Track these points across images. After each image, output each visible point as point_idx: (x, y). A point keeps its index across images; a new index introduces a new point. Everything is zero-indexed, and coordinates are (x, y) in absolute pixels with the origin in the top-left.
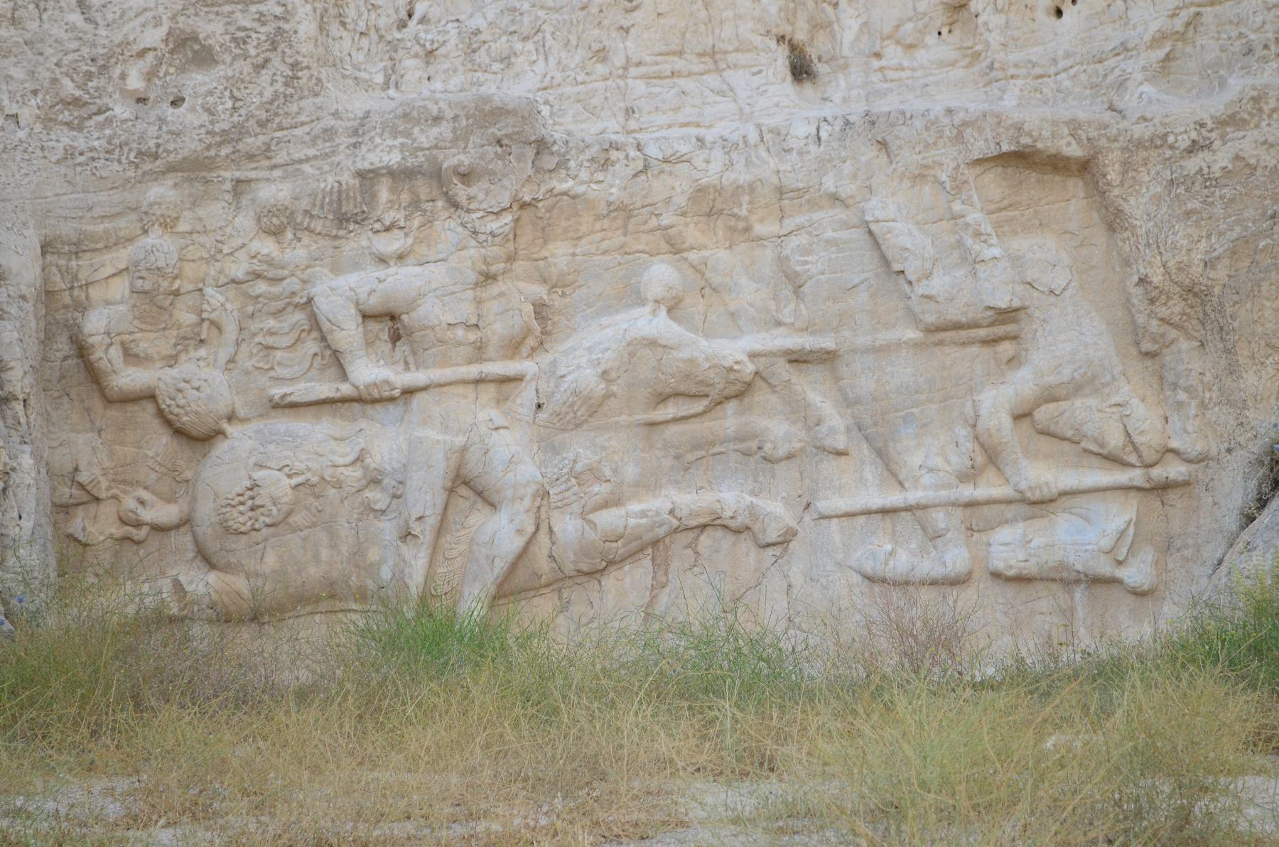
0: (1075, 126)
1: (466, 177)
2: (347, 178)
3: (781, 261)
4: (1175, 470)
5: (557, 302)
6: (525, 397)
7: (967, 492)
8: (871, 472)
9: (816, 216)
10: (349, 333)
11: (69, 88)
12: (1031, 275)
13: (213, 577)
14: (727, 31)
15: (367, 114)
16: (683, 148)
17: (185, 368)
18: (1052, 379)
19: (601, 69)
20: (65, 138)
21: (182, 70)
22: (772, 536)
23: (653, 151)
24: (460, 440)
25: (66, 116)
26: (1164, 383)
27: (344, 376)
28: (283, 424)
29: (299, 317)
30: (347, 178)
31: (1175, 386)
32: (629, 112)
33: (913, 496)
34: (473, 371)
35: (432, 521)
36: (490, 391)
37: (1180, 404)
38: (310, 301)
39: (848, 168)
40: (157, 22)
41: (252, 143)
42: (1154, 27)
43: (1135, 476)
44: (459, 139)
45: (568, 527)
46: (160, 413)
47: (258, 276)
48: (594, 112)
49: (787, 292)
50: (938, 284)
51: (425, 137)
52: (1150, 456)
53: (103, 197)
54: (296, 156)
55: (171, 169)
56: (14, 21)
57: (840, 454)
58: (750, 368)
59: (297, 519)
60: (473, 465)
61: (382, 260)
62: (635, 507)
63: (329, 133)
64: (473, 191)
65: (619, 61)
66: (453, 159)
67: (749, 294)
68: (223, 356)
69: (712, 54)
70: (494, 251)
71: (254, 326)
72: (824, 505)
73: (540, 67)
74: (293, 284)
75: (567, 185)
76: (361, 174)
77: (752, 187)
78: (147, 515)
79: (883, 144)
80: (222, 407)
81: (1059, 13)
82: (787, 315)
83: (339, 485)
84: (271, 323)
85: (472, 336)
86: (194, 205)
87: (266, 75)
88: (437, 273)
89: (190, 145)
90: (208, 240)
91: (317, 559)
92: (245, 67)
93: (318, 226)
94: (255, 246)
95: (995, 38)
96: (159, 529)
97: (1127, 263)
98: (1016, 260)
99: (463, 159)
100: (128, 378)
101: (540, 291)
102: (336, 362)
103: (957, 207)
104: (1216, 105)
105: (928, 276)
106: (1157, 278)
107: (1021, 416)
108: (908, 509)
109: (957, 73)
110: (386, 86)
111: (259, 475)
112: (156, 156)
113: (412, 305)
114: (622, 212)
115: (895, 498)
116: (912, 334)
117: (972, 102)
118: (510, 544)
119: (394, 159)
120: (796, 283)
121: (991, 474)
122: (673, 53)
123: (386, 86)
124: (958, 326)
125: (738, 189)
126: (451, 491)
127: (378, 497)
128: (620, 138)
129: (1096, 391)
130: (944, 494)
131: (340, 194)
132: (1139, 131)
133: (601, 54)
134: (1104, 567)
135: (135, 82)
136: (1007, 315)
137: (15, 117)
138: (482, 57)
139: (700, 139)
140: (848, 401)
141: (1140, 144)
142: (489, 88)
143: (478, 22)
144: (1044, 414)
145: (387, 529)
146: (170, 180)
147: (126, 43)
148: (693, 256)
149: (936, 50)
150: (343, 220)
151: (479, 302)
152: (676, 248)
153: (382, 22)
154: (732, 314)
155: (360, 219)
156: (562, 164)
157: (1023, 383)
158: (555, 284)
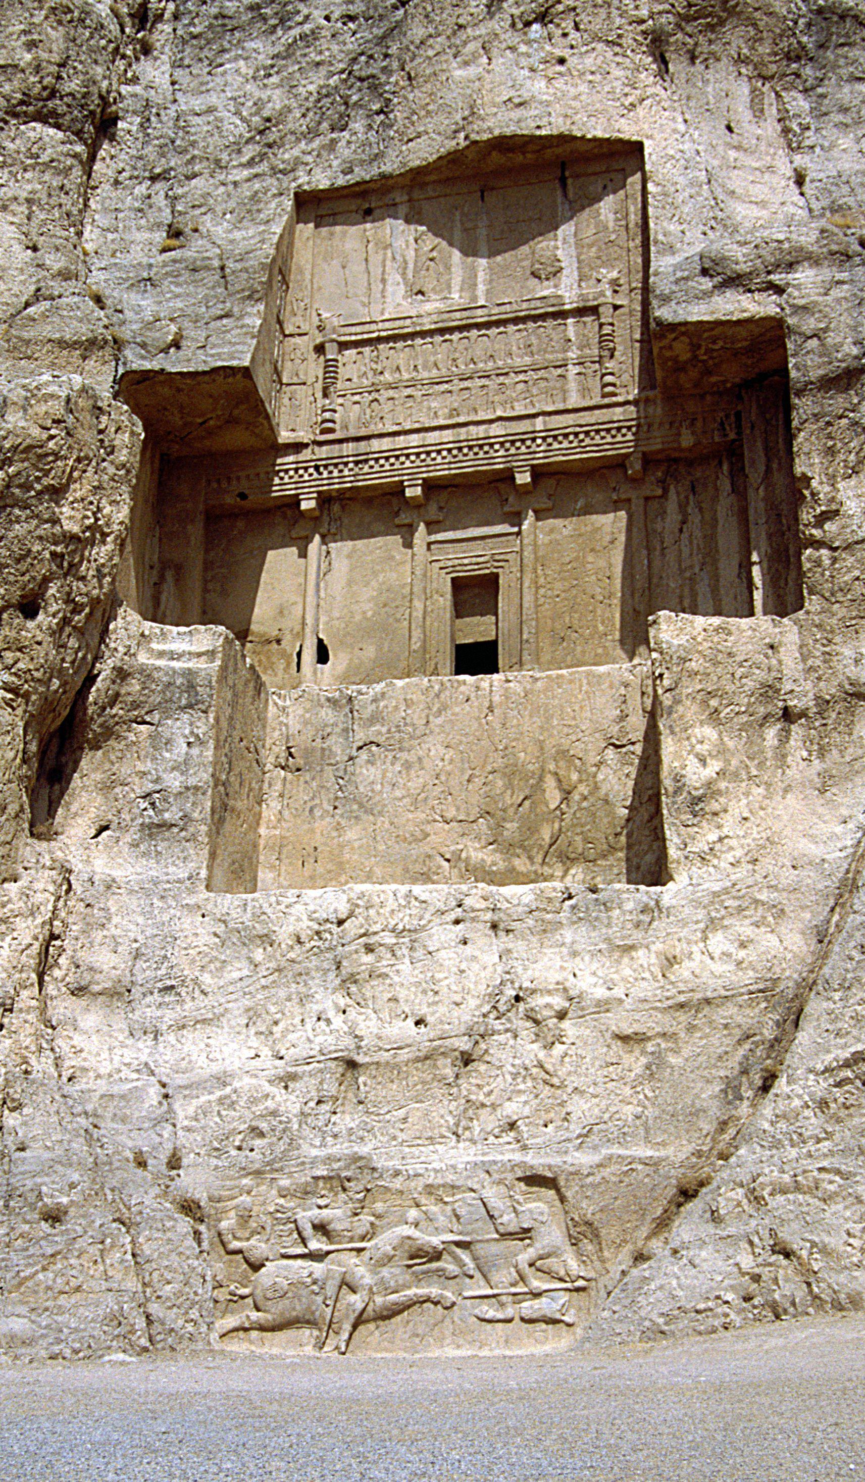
0: (550, 1167)
1: (349, 1180)
2: (309, 1179)
3: (454, 1210)
4: (581, 1283)
5: (377, 1222)
6: (366, 1255)
7: (513, 1290)
8: (482, 1282)
9: (465, 1195)
10: (308, 1231)
11: (216, 1144)
12: (535, 1216)
13: (260, 1314)
14: (436, 1131)
15: (316, 1157)
16: (421, 1171)
17: (253, 1242)
18: (541, 1252)
19: (394, 1143)
20: (215, 1161)
21: (253, 1138)
22: (448, 1305)
23: (411, 1172)
24: (344, 1269)
25: (215, 1154)
26: (579, 1254)
27: (306, 1246)
28: (285, 1262)
29: (292, 1225)
30: (309, 1179)
31: (582, 1255)
32: (403, 1158)
33: (496, 1291)
34: (350, 1246)
35: (334, 1298)
36: (354, 1253)
37: (584, 1262)
38: (295, 1221)
39: (476, 1179)
40: (245, 1122)
41: (277, 1166)
42: (577, 1132)
43: (569, 1285)
44: (347, 1167)
45: (379, 1300)
46: (244, 1258)
47: (278, 1211)
48: (392, 1158)
49: (454, 1220)
50: (505, 1219)
51: (336, 1166)
52: (574, 1278)
53: (228, 1183)
54: (293, 1169)
55: (250, 1174)
56: (197, 1120)
57: (471, 1277)
58: (441, 1247)
59: (290, 1294)
60: (348, 1279)
61: (320, 1207)
62: (402, 1294)
63: (303, 1163)
64: (351, 1184)
65: (400, 1140)
66: (344, 1174)
67: (442, 1221)
68: (265, 1238)
69: (431, 1138)
70: (358, 1205)
71: (276, 1228)
72: (466, 1294)
73: (374, 1141)
74: (289, 1214)
75: (383, 1183)
76: (313, 1178)
77: (443, 1186)
78: (239, 1292)
79: (488, 1172)
80: (264, 1256)
81: (546, 1126)
82: (455, 1230)
83: (303, 1283)
84: (281, 1227)
85: (349, 1234)
86: (258, 1185)
87: (281, 1142)
88: (338, 1212)
89: (257, 1166)
90: (261, 1198)
91: (294, 1309)
92: (275, 1139)
93: (299, 1195)
94: (277, 1201)
95: (525, 1136)
96: (242, 1297)
97: (566, 1212)
98: (531, 1211)
99: (348, 1174)
100: (235, 1245)
101: (372, 1219)
102: (304, 1241)
103: (512, 1193)
104: (596, 1158)
105: (501, 1216)
106: (577, 1219)
107: (531, 1265)
108: (494, 1296)
109: (512, 1146)
110: (321, 1146)
111: (277, 1279)
112: (244, 1169)
113: (329, 1223)
114: (402, 1192)
115: (489, 1292)
116: (496, 1236)
117: (517, 1157)
118: (360, 1306)
119: (325, 1173)
120: (458, 1217)
121: (521, 1283)
122: (419, 1138)
123: (321, 1146)
124: (511, 1234)
125: (439, 1186)
126: (340, 1287)
127: (315, 1288)
128: (400, 1167)
129: (556, 1256)
130: (505, 1291)
131: (307, 1183)
132: (572, 1169)
133: (395, 1138)
134: (558, 1316)
135: (237, 1143)
136: (528, 1230)
137: (198, 1154)
138: (353, 1138)
139: (427, 1169)
140: (475, 1259)
141: (572, 1174)
142: (356, 1149)
143: (352, 1125)
144: (538, 1263)
145: (319, 1299)
146: (250, 1177)
147: (234, 1129)
148: (424, 1208)
150: (307, 1193)
151: (352, 1222)
153: (320, 1124)
154: (436, 1229)
155: (313, 1193)
156: (381, 1176)
157: (531, 1253)
158: (378, 1217)
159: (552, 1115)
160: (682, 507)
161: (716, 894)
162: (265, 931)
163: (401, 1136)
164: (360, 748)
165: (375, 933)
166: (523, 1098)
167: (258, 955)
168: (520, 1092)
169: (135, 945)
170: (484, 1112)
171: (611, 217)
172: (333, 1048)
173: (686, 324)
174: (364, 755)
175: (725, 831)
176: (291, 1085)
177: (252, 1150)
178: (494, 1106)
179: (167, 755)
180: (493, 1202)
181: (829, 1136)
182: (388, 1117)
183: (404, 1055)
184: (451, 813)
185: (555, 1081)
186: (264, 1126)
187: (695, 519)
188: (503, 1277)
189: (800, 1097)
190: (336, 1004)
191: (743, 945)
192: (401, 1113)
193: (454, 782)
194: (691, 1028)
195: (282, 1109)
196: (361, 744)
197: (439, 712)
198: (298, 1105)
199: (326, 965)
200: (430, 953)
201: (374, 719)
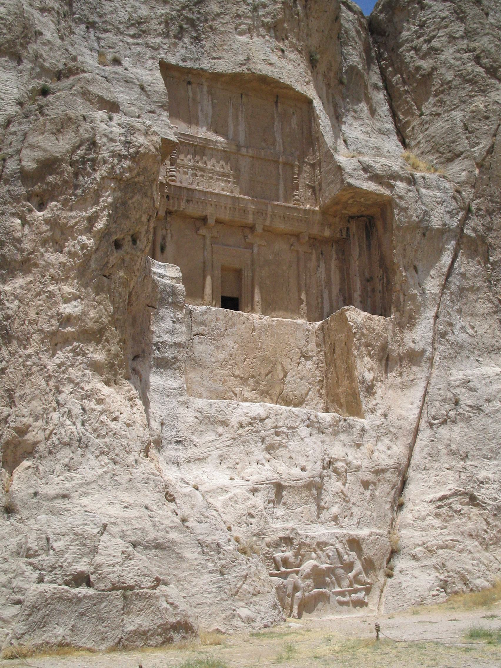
6: (300, 574)
8: (336, 585)
27: (278, 569)
44: (291, 533)
45: (307, 594)
63: (273, 531)
67: (323, 558)
69: (312, 521)
89: (257, 531)
119: (284, 535)
120: (329, 557)
133: (300, 521)
143: (282, 514)
149: (333, 523)
150: (277, 545)
152: (315, 551)
159: (346, 514)
160: (318, 260)
161: (378, 427)
162: (224, 419)
163: (303, 520)
164: (195, 335)
165: (280, 427)
166: (337, 505)
167: (220, 429)
168: (336, 502)
169: (162, 418)
170: (325, 510)
171: (296, 126)
172: (272, 478)
173: (361, 188)
174: (197, 339)
175: (377, 401)
176: (256, 494)
177: (251, 524)
178: (328, 509)
179: (163, 325)
180: (342, 550)
181: (446, 527)
182: (296, 511)
183: (300, 483)
184: (237, 373)
185: (347, 499)
186: (252, 512)
187: (322, 265)
188: (346, 583)
189: (425, 511)
190: (265, 458)
191: (389, 449)
192: (300, 509)
193: (238, 359)
194: (379, 481)
195: (257, 505)
196: (195, 333)
197: (231, 325)
198: (262, 503)
199: (257, 439)
200: (302, 439)
201: (202, 323)
